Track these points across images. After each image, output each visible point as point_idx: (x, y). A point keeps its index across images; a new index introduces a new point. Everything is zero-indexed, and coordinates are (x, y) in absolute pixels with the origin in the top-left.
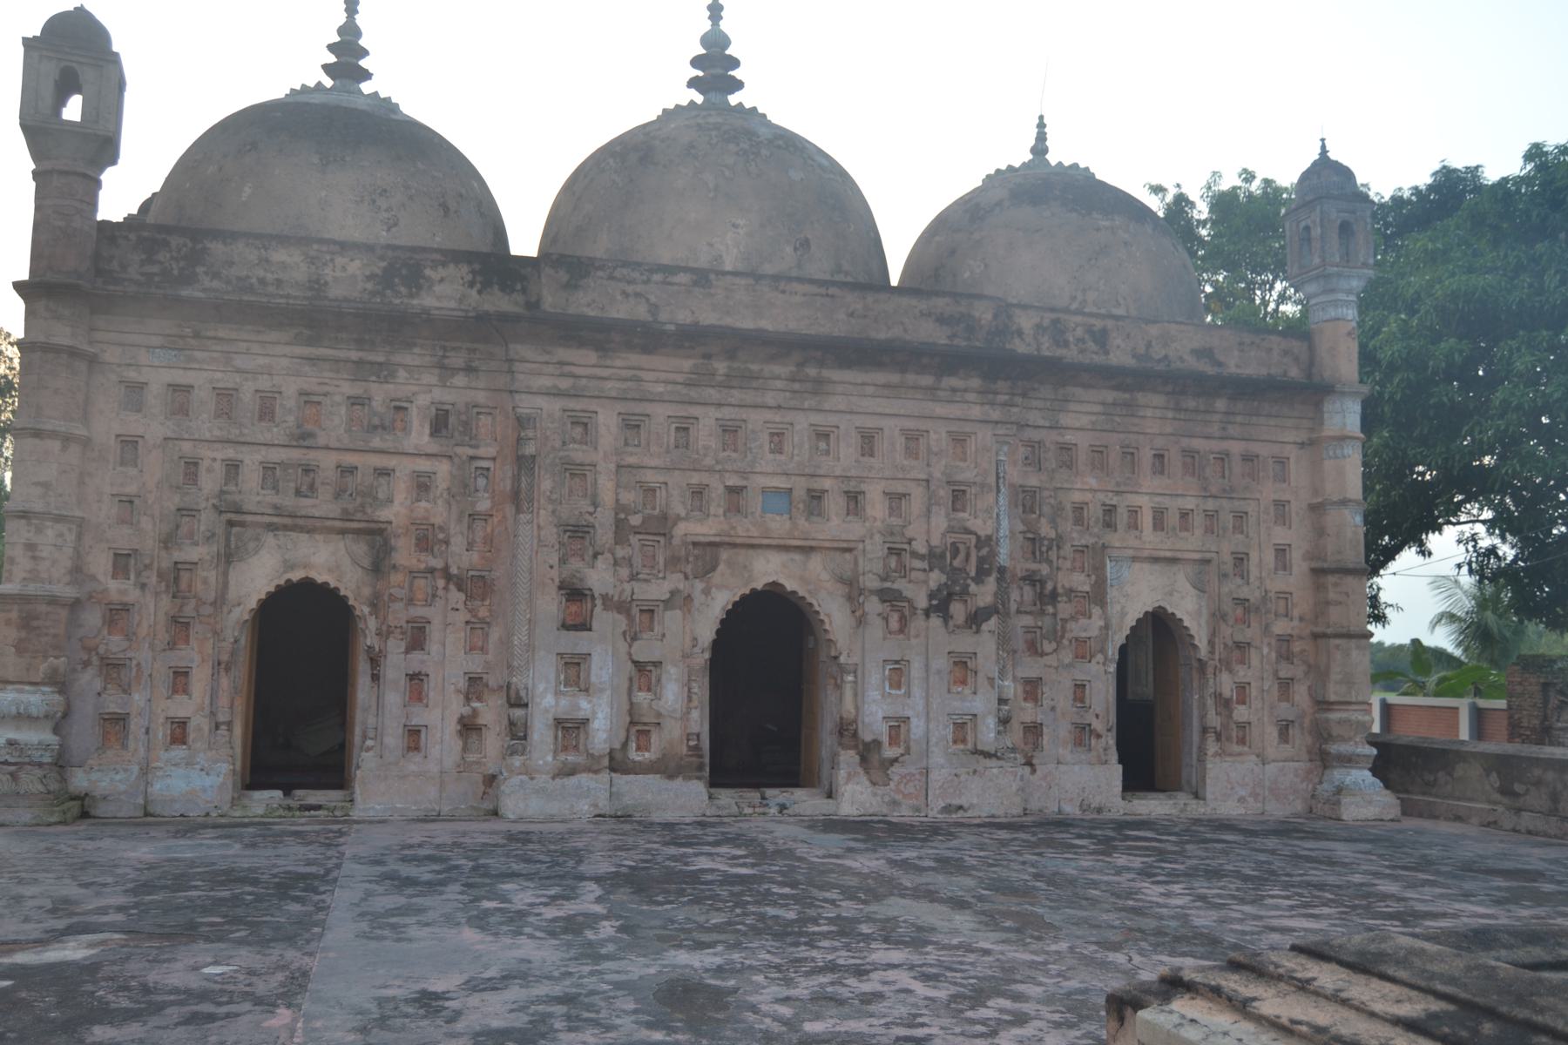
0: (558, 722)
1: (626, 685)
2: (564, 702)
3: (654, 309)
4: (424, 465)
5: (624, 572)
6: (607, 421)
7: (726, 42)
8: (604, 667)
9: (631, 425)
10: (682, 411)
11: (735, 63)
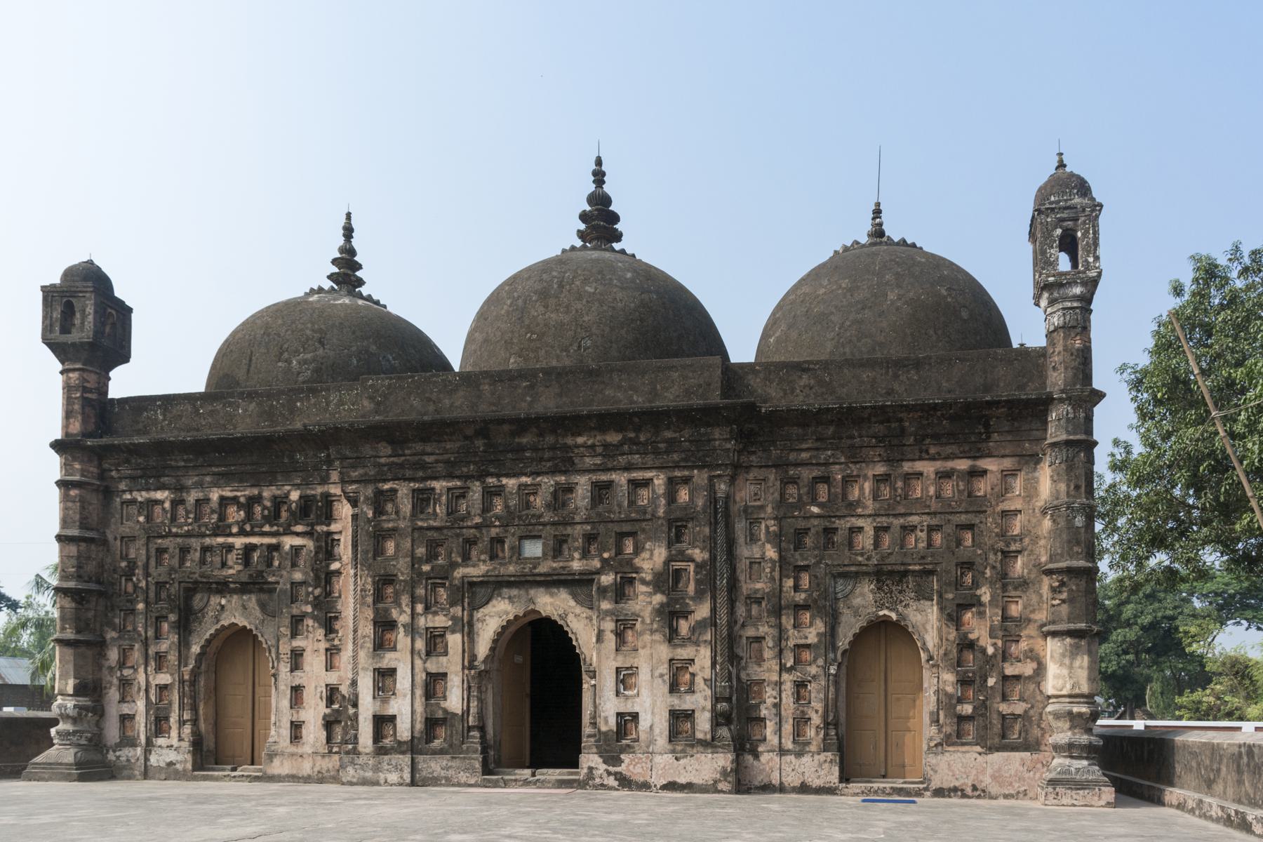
4: (298, 541)
5: (420, 608)
8: (403, 681)
9: (422, 499)
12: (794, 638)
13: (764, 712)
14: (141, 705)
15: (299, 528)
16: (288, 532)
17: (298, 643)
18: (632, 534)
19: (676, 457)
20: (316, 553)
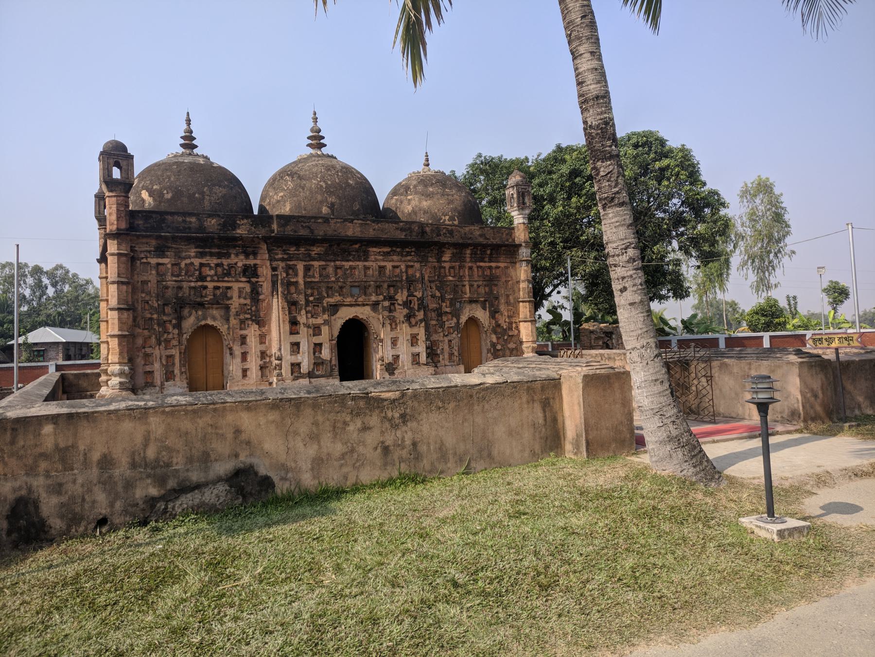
0: (292, 365)
1: (312, 351)
2: (293, 357)
3: (312, 231)
5: (309, 315)
6: (300, 267)
7: (320, 131)
8: (304, 347)
9: (307, 269)
10: (323, 263)
11: (323, 138)
12: (447, 324)
13: (439, 352)
14: (157, 366)
15: (244, 279)
16: (237, 281)
17: (243, 332)
18: (393, 286)
19: (409, 258)
20: (252, 291)
